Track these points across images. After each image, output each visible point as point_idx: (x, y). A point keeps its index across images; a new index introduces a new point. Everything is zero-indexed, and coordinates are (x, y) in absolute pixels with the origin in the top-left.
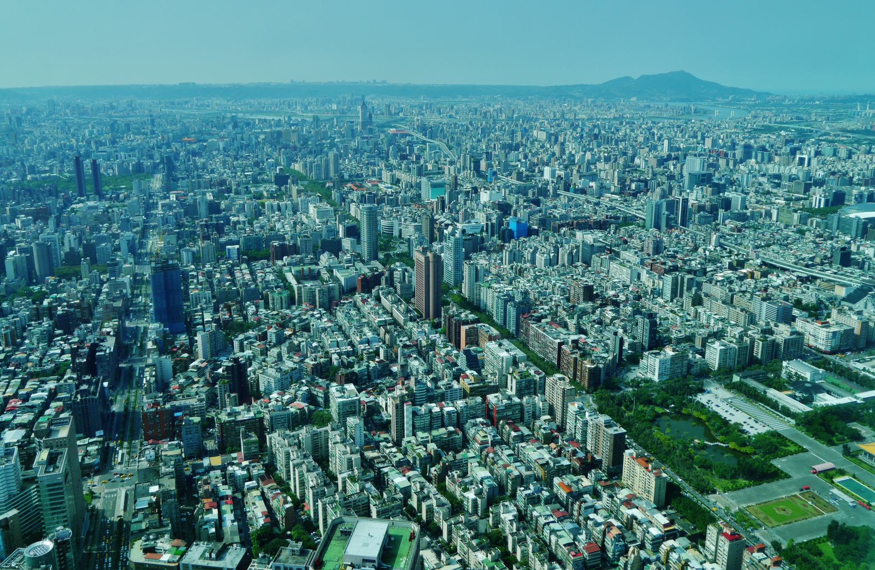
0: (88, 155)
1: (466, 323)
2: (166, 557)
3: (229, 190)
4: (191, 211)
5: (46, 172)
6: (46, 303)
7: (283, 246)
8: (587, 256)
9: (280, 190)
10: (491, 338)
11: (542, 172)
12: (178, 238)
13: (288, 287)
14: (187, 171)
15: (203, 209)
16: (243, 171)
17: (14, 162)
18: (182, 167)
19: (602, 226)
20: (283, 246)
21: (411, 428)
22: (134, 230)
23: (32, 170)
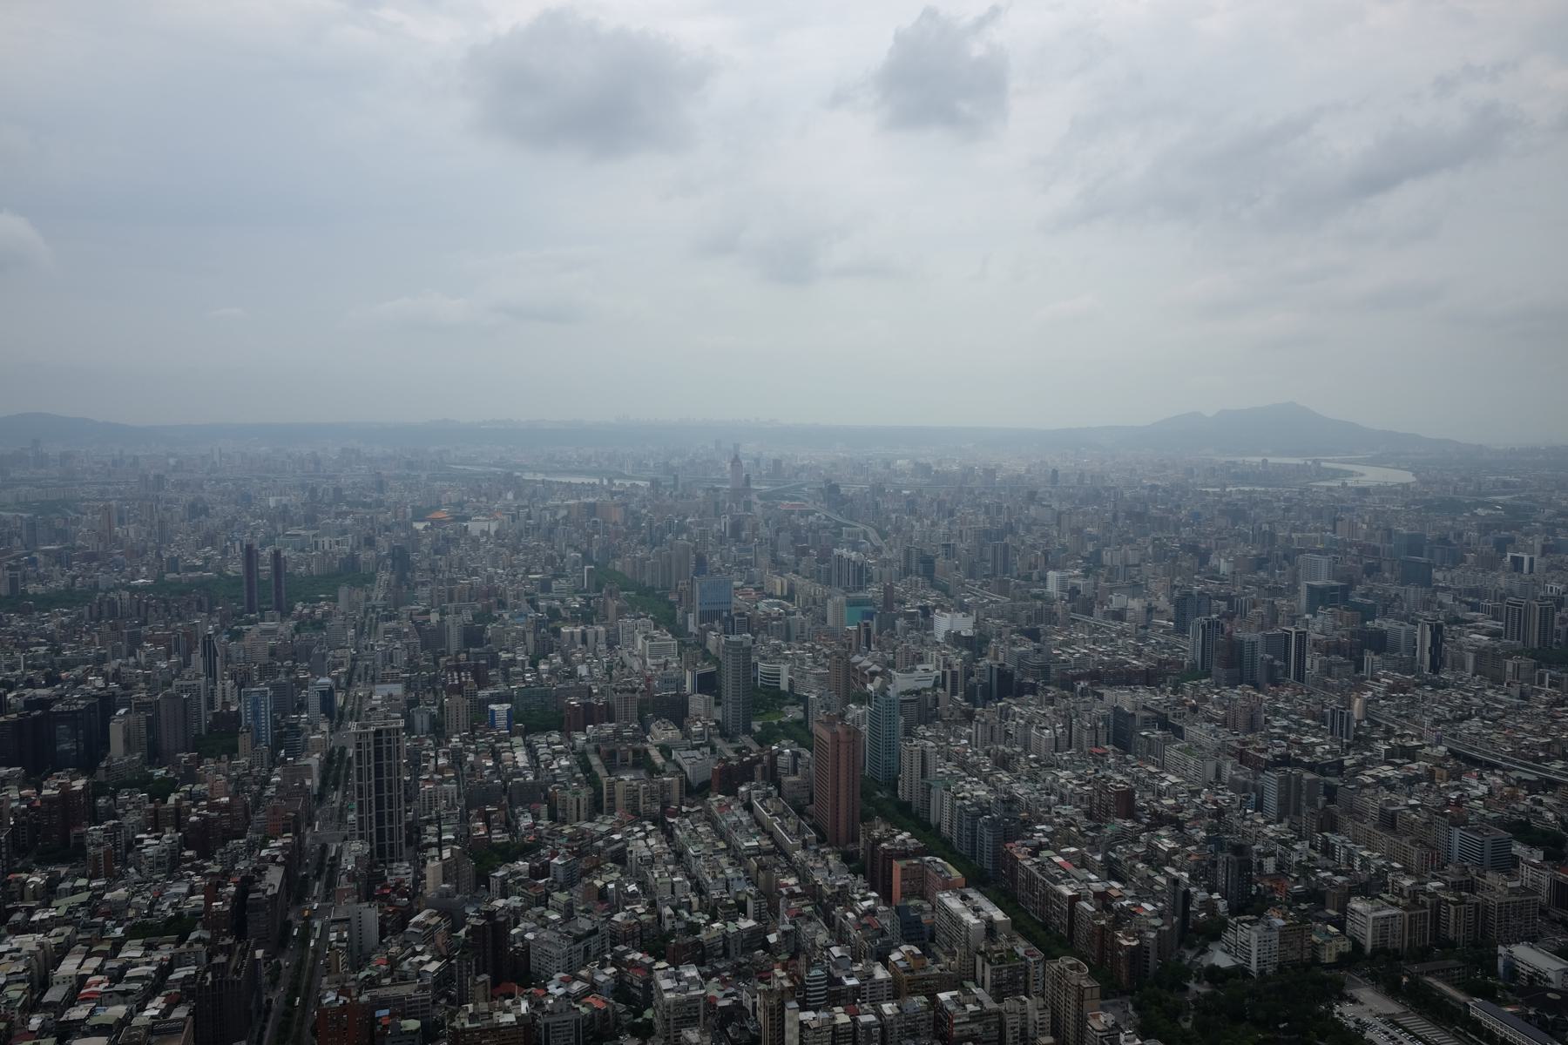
0: (269, 540)
1: (905, 855)
3: (502, 604)
4: (432, 639)
5: (194, 568)
6: (172, 799)
7: (588, 707)
8: (1121, 733)
9: (588, 605)
10: (948, 886)
11: (1044, 579)
12: (408, 688)
13: (592, 780)
14: (433, 571)
16: (528, 572)
17: (145, 552)
18: (425, 565)
19: (1149, 678)
20: (588, 707)
22: (334, 673)
23: (173, 564)
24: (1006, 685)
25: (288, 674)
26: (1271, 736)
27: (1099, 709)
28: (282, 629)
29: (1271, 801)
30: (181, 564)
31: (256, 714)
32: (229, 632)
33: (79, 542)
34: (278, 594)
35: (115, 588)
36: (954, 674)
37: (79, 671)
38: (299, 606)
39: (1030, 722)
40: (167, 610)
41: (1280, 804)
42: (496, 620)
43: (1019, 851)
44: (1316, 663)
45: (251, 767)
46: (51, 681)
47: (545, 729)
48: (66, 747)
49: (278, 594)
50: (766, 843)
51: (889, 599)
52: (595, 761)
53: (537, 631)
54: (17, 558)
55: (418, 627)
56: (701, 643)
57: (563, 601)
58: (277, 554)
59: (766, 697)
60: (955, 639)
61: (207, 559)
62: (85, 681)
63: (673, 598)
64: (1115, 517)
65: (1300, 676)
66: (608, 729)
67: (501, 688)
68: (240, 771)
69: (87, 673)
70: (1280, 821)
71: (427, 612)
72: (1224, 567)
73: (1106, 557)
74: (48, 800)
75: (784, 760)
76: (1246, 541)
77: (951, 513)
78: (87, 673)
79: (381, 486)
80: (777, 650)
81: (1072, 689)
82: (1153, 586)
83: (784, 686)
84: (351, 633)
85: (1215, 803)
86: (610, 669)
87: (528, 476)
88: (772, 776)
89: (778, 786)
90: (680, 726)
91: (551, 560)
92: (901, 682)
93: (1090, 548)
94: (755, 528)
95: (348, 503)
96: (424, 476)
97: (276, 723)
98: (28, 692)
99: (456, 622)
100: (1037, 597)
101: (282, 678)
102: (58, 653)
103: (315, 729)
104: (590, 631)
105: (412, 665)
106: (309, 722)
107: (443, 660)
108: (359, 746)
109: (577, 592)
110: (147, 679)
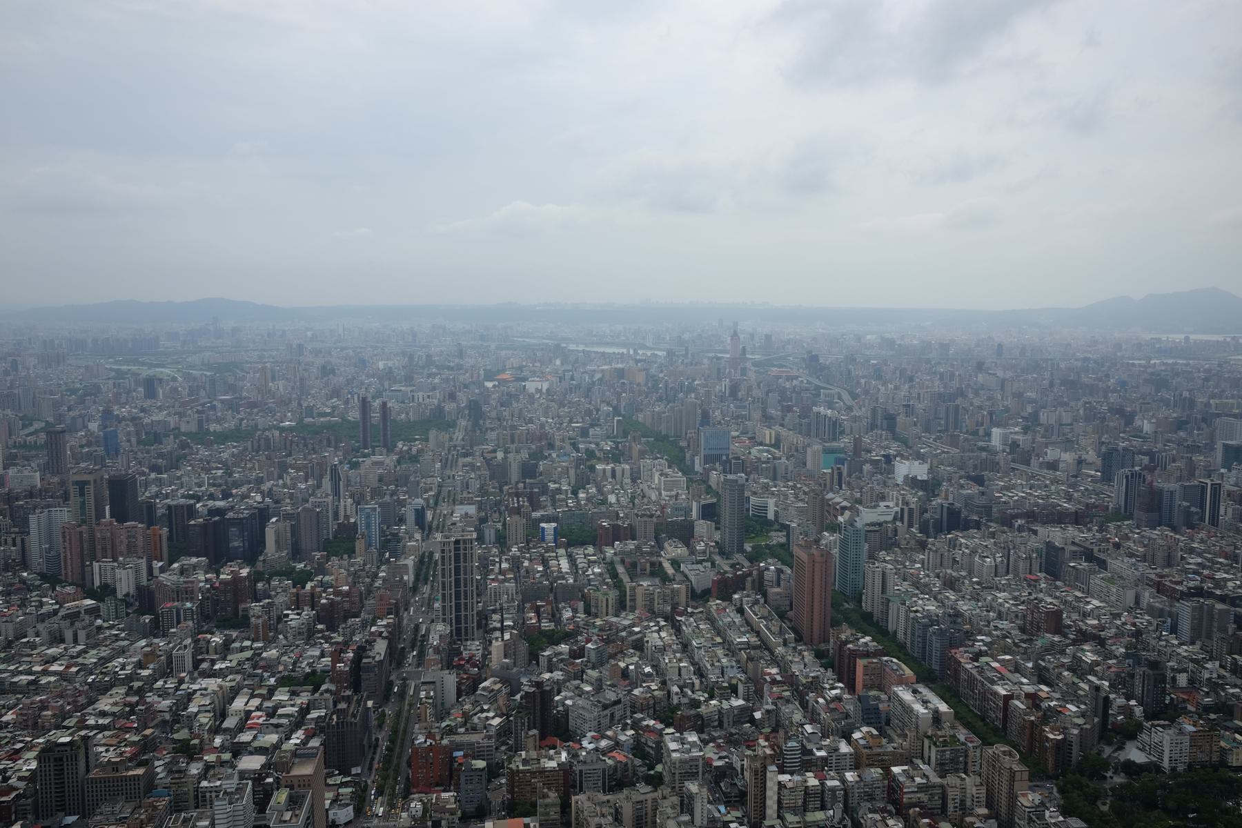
0: (378, 394)
1: (867, 655)
3: (551, 446)
4: (498, 472)
5: (325, 415)
6: (309, 586)
7: (616, 528)
8: (1052, 562)
9: (617, 448)
10: (902, 681)
11: (988, 434)
12: (480, 509)
13: (618, 585)
15: (514, 474)
16: (571, 421)
18: (494, 414)
19: (1077, 519)
20: (616, 528)
22: (425, 496)
23: (310, 411)
24: (954, 520)
25: (392, 495)
26: (1186, 571)
27: (1034, 543)
28: (387, 461)
29: (1185, 625)
30: (315, 411)
31: (368, 525)
32: (349, 463)
33: (245, 394)
34: (385, 435)
35: (269, 429)
36: (911, 511)
37: (244, 489)
38: (400, 444)
39: (974, 552)
40: (306, 445)
41: (1193, 629)
42: (546, 458)
43: (962, 656)
44: (1230, 511)
45: (365, 565)
46: (226, 495)
47: (583, 544)
48: (236, 544)
49: (385, 435)
50: (754, 640)
51: (858, 448)
52: (621, 569)
53: (577, 467)
54: (203, 405)
55: (488, 462)
56: (705, 480)
57: (597, 445)
58: (384, 404)
59: (756, 524)
60: (913, 482)
61: (334, 408)
62: (248, 497)
63: (683, 444)
64: (1052, 385)
65: (1214, 521)
66: (631, 545)
67: (550, 511)
68: (357, 567)
69: (250, 490)
70: (1193, 643)
71: (494, 451)
72: (1147, 427)
73: (1043, 417)
74: (223, 582)
75: (768, 576)
76: (1168, 405)
77: (911, 379)
78: (250, 490)
79: (461, 354)
80: (766, 487)
81: (1011, 526)
82: (1083, 442)
83: (771, 516)
84: (438, 465)
85: (1134, 625)
86: (633, 498)
87: (572, 347)
88: (760, 587)
89: (765, 595)
90: (687, 545)
91: (589, 413)
92: (867, 516)
93: (1029, 409)
94: (750, 389)
95: (437, 367)
96: (493, 347)
97: (382, 533)
99: (515, 461)
100: (982, 449)
101: (387, 498)
102: (230, 475)
103: (411, 537)
104: (618, 469)
105: (483, 491)
106: (407, 532)
107: (506, 488)
108: (443, 551)
109: (608, 437)
110: (291, 496)
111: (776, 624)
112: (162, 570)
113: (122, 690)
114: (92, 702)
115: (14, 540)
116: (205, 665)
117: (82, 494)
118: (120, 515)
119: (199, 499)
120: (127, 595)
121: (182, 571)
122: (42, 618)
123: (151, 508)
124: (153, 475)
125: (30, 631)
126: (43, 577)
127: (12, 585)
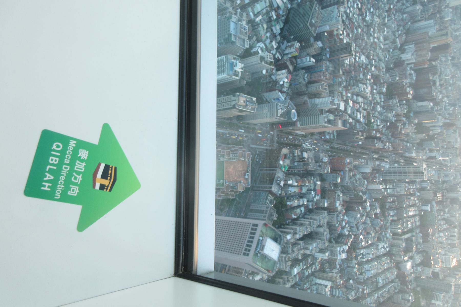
2: (281, 162)
6: (404, 119)
12: (436, 181)
13: (404, 233)
15: (452, 195)
20: (428, 234)
21: (319, 283)
37: (444, 91)
46: (441, 85)
50: (380, 285)
62: (441, 94)
74: (406, 89)
83: (433, 301)
86: (441, 243)
88: (401, 291)
89: (398, 293)
98: (438, 81)
102: (450, 86)
104: (455, 238)
107: (446, 191)
111: (386, 295)
112: (411, 68)
113: (367, 63)
114: (364, 54)
115: (423, 17)
116: (375, 87)
117: (442, 35)
118: (434, 50)
119: (440, 76)
120: (401, 58)
121: (410, 74)
122: (394, 33)
123: (436, 60)
124: (450, 58)
125: (389, 30)
126: (409, 29)
127: (405, 20)
